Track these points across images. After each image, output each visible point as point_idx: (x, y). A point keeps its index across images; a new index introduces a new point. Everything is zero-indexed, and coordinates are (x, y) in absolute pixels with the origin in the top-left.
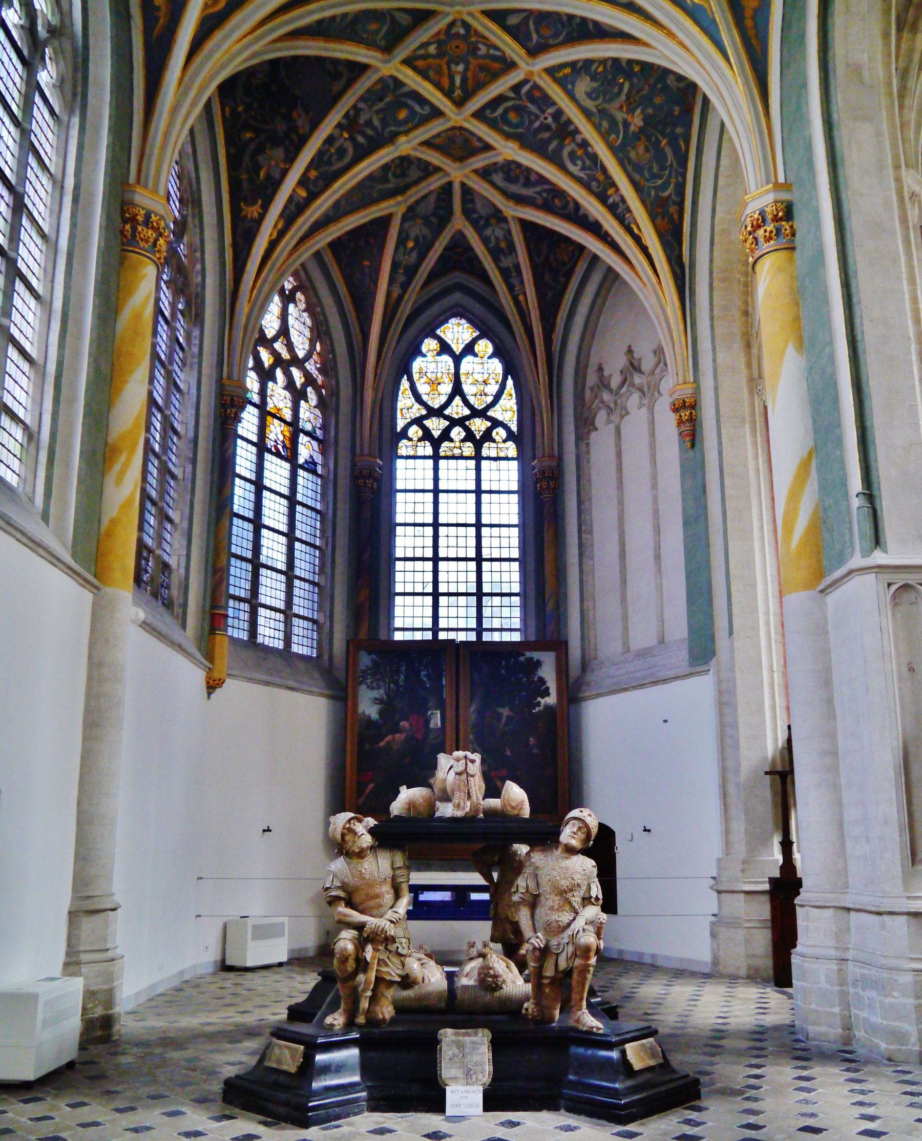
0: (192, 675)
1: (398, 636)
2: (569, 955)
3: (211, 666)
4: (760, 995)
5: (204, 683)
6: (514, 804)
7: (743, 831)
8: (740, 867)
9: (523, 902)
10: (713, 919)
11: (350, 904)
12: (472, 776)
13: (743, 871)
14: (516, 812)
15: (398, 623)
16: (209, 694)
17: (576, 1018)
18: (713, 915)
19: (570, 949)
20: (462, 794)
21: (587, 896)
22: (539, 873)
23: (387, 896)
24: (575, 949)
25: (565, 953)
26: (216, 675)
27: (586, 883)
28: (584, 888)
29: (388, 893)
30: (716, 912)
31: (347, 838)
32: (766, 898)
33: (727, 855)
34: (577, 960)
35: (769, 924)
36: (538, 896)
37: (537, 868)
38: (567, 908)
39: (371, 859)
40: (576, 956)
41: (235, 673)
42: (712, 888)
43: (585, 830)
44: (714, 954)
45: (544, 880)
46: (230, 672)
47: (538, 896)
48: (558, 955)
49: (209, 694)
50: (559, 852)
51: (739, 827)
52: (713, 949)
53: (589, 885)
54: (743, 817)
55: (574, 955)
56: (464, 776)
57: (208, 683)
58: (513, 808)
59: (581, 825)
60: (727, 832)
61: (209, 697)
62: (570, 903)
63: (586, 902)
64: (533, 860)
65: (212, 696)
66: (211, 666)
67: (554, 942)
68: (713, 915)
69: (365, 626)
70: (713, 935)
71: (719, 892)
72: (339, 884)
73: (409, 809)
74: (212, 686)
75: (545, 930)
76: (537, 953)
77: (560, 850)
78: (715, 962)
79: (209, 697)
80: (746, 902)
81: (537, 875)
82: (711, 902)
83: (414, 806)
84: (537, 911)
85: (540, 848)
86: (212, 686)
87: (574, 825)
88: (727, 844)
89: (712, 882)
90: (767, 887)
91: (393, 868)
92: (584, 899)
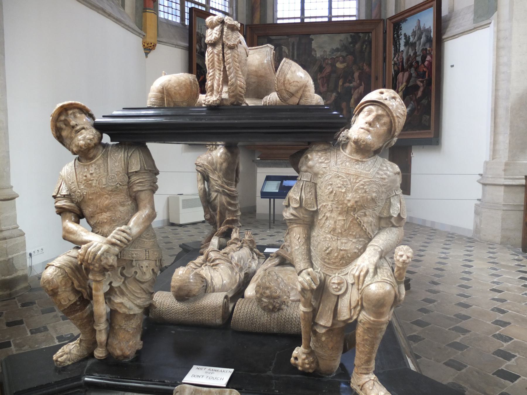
0: (133, 42)
1: (279, 22)
2: (353, 305)
3: (144, 34)
4: (517, 263)
5: (142, 45)
6: (292, 89)
7: (508, 141)
8: (503, 167)
9: (296, 220)
10: (478, 202)
11: (79, 216)
12: (232, 48)
13: (505, 170)
14: (294, 101)
15: (279, 16)
16: (147, 54)
17: (361, 383)
18: (478, 200)
19: (353, 296)
20: (217, 72)
21: (385, 215)
22: (319, 181)
23: (121, 209)
24: (362, 298)
25: (347, 296)
26: (149, 40)
27: (384, 196)
28: (381, 204)
29: (122, 205)
30: (480, 198)
31: (64, 133)
32: (523, 189)
33: (493, 159)
34: (363, 313)
35: (522, 208)
36: (316, 212)
37: (316, 174)
38: (356, 230)
39: (100, 161)
40: (362, 307)
41: (164, 40)
42: (479, 182)
43: (385, 120)
44: (477, 226)
45: (323, 191)
46: (161, 40)
47: (316, 212)
48: (338, 297)
49: (147, 54)
50: (346, 153)
51: (504, 139)
52: (475, 222)
53: (388, 199)
54: (508, 132)
55: (361, 305)
56: (219, 48)
57: (144, 46)
58: (292, 95)
59: (380, 112)
60: (495, 143)
61: (147, 56)
62: (359, 224)
63: (383, 224)
64: (310, 163)
65: (149, 55)
66: (144, 34)
67: (334, 279)
68: (478, 200)
69: (257, 15)
70: (477, 213)
71: (484, 185)
72: (64, 192)
73: (162, 99)
74: (148, 49)
75: (323, 259)
76: (309, 295)
77: (348, 149)
78: (477, 230)
79: (147, 56)
80: (505, 192)
81: (316, 184)
82: (477, 191)
83: (169, 95)
84: (314, 234)
85: (322, 146)
86: (148, 49)
87: (370, 112)
88: (494, 151)
89: (479, 177)
90: (523, 182)
91: (128, 173)
92: (380, 218)
